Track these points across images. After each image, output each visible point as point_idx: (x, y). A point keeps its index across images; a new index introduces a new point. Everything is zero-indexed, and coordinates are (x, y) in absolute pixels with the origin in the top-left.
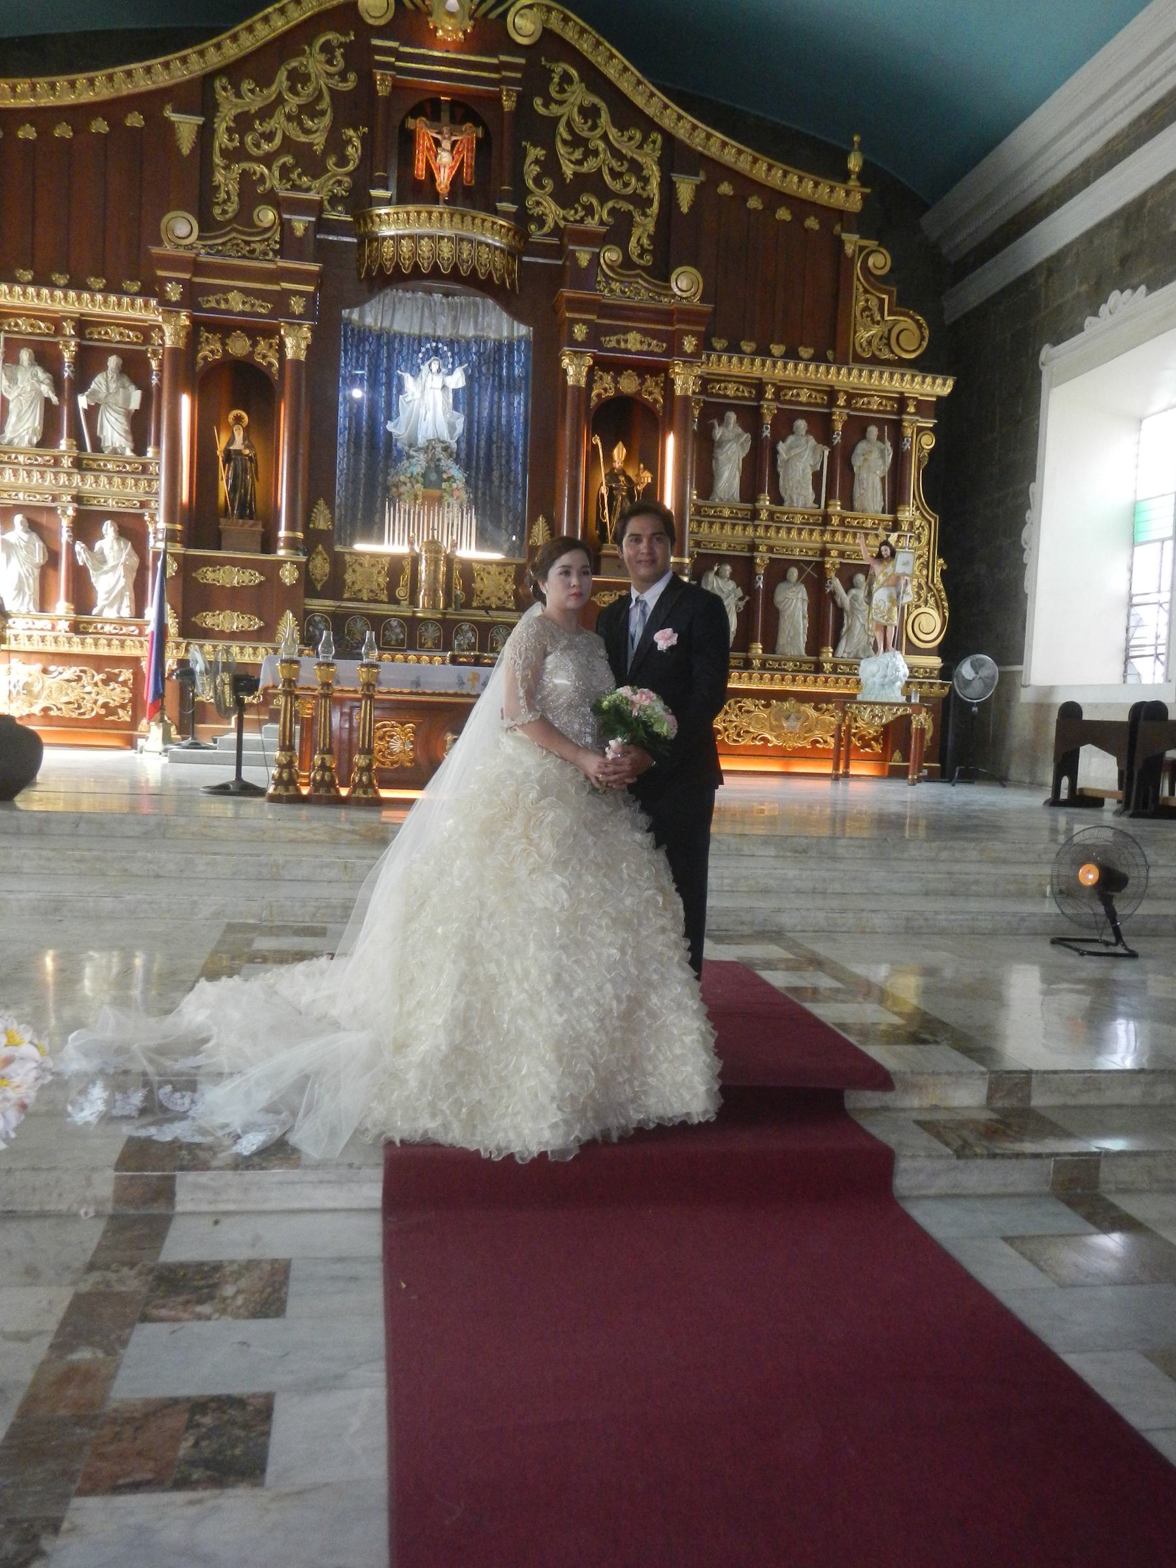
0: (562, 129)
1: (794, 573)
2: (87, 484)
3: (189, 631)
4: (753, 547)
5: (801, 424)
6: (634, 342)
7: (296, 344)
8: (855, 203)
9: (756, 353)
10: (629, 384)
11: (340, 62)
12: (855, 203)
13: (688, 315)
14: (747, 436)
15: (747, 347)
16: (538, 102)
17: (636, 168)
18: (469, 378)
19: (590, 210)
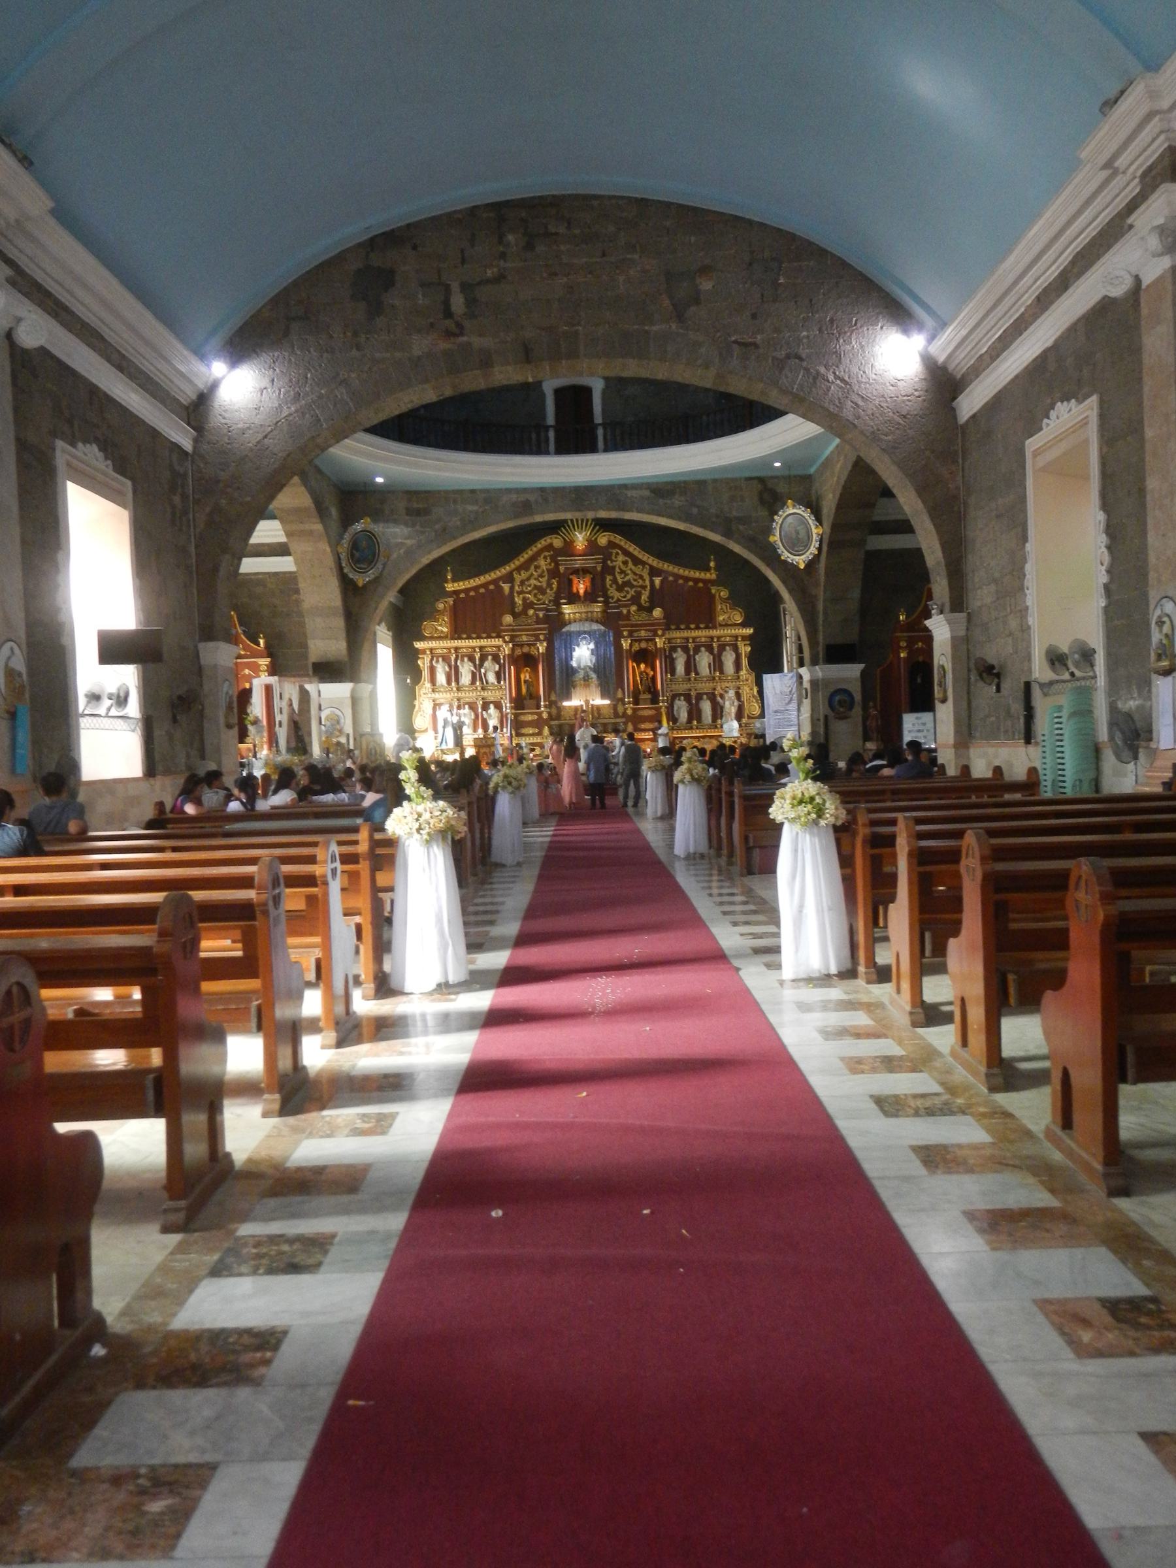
0: (617, 570)
1: (705, 697)
2: (485, 694)
3: (519, 735)
5: (703, 649)
8: (714, 576)
10: (643, 645)
11: (548, 561)
12: (714, 576)
13: (659, 624)
15: (682, 627)
16: (609, 562)
17: (641, 577)
19: (628, 592)
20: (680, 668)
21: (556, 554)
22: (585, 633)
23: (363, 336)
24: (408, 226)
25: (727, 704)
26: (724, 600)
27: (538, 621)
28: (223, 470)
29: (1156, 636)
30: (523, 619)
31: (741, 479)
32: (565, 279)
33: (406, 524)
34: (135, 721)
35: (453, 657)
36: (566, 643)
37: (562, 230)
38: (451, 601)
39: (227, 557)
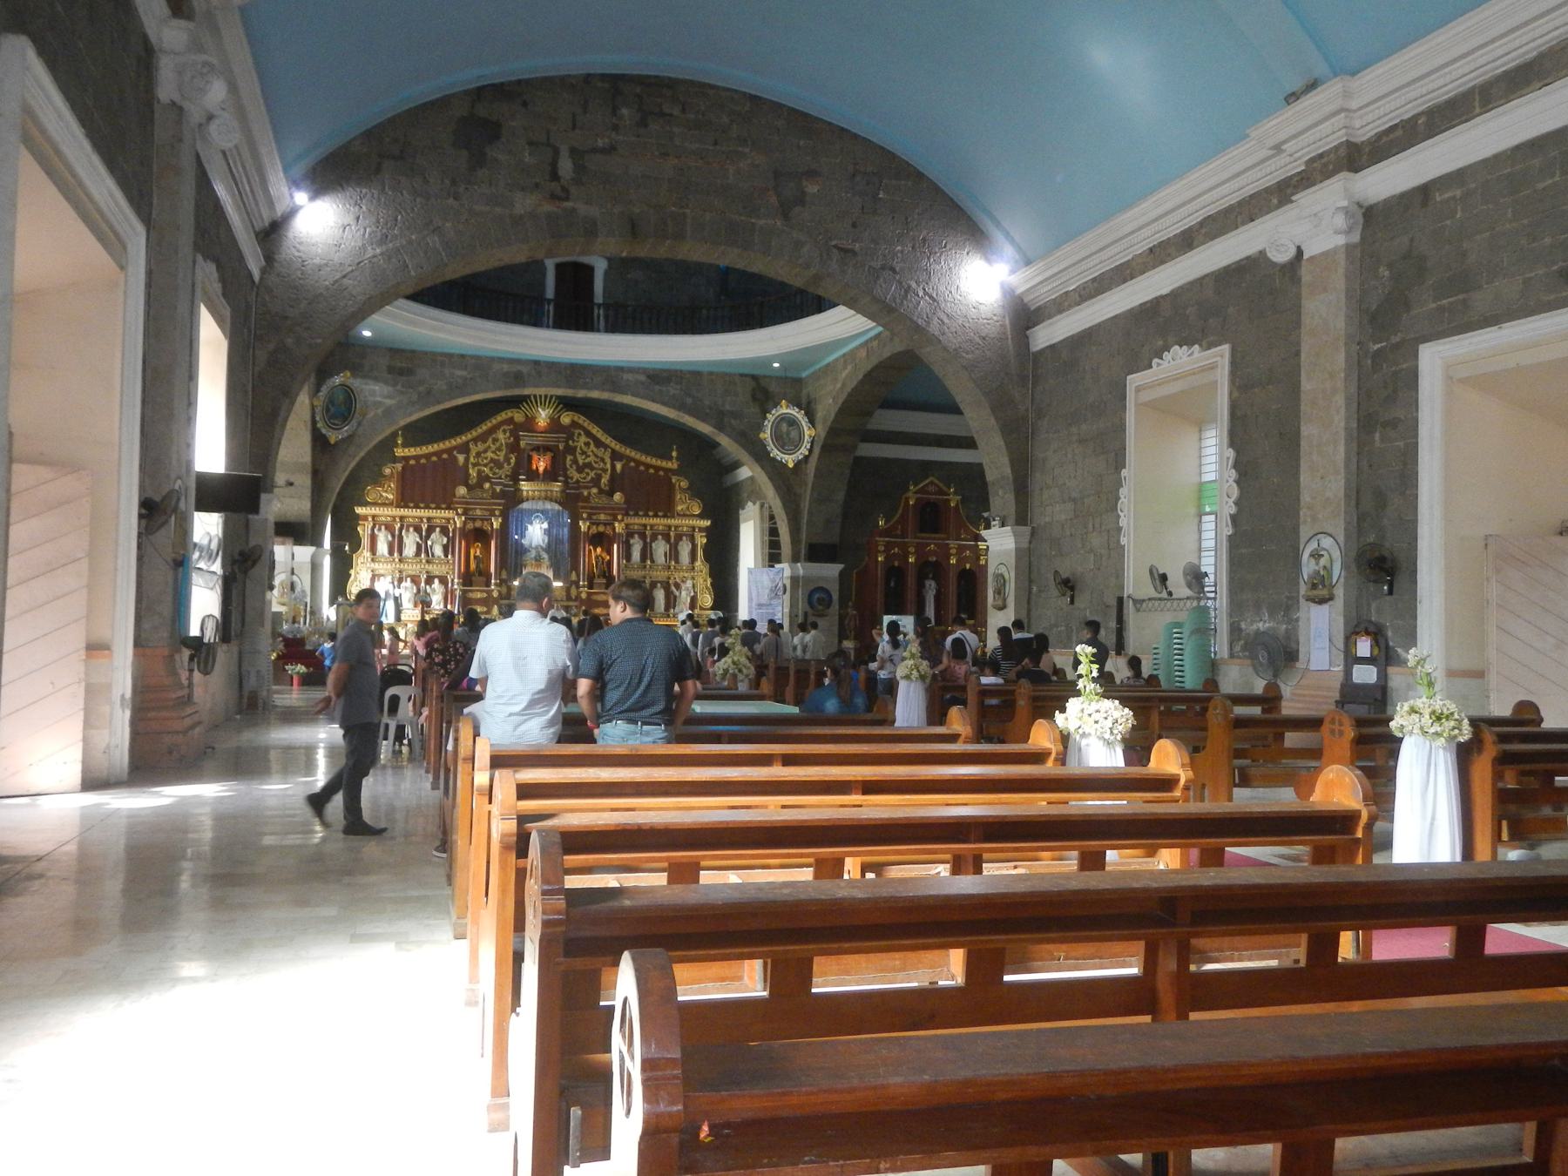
1: (659, 585)
2: (430, 567)
4: (645, 577)
5: (660, 537)
6: (602, 517)
7: (496, 524)
9: (644, 516)
10: (601, 529)
11: (508, 434)
13: (619, 509)
14: (641, 542)
15: (641, 513)
16: (571, 442)
17: (603, 460)
18: (549, 524)
19: (588, 474)
20: (636, 555)
21: (516, 429)
22: (538, 511)
23: (463, 186)
24: (519, 82)
25: (684, 593)
26: (683, 490)
27: (494, 495)
28: (292, 307)
29: (1308, 567)
30: (479, 493)
31: (735, 375)
32: (676, 161)
33: (386, 383)
34: (215, 578)
35: (397, 526)
36: (517, 517)
37: (676, 112)
38: (399, 466)
39: (287, 401)
